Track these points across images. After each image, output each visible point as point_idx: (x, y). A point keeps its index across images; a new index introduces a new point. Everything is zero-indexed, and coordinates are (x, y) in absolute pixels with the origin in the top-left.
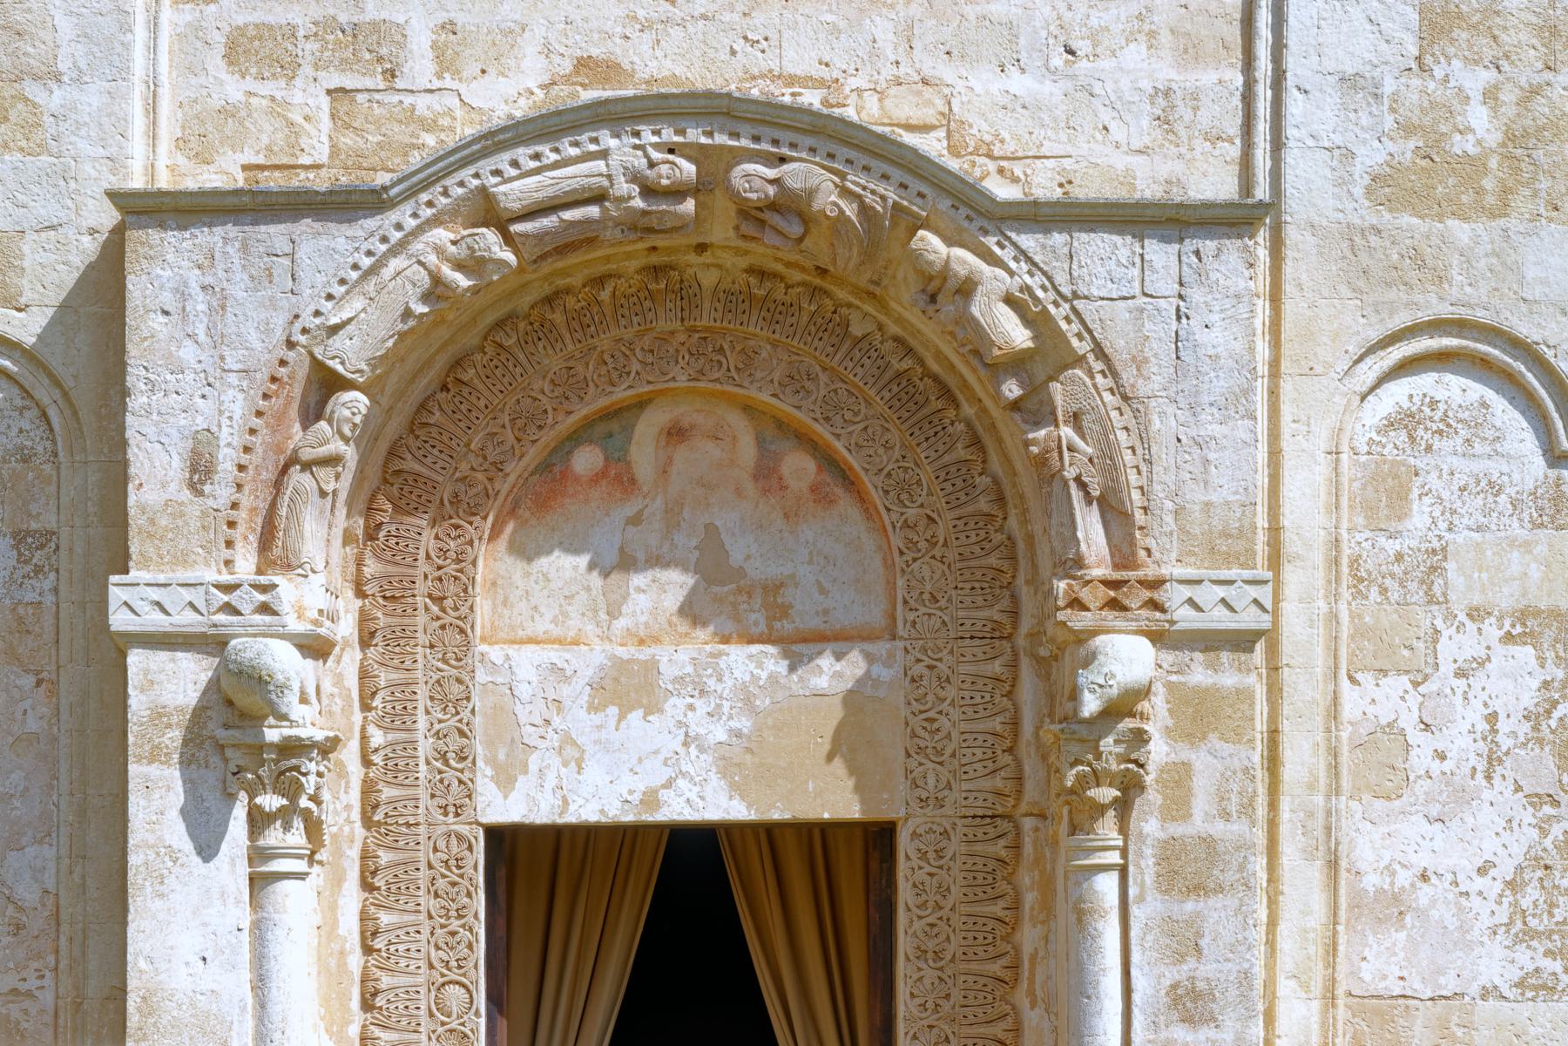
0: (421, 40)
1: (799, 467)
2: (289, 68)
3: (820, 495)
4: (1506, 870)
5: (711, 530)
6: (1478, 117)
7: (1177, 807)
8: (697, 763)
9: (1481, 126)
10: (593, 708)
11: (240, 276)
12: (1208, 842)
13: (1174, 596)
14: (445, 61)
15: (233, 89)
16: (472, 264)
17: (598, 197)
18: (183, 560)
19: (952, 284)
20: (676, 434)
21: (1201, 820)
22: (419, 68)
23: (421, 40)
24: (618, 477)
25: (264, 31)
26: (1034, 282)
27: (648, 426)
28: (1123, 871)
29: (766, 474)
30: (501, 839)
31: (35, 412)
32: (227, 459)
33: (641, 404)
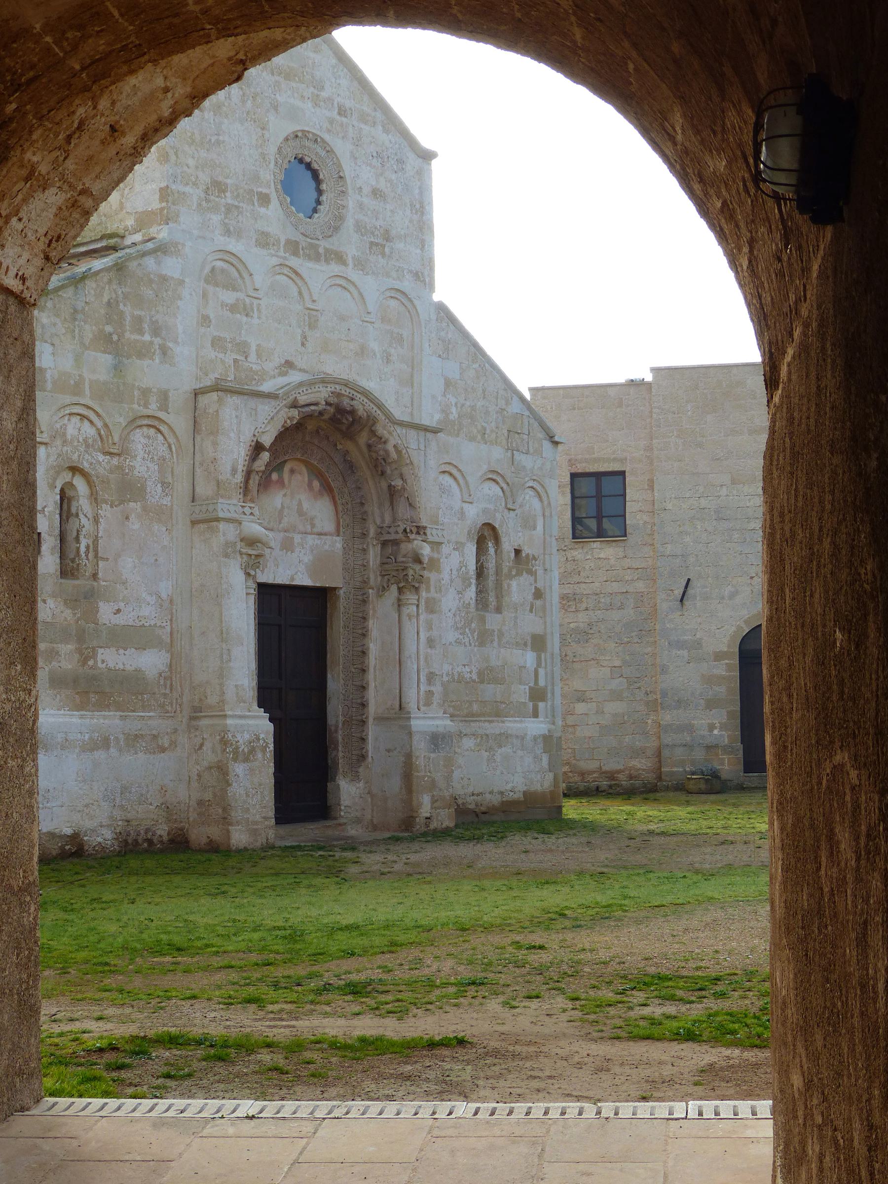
0: (254, 348)
1: (316, 484)
2: (224, 350)
4: (453, 611)
5: (300, 500)
6: (454, 410)
7: (428, 590)
9: (454, 413)
10: (281, 550)
11: (244, 414)
12: (434, 599)
13: (428, 532)
14: (259, 356)
15: (212, 354)
17: (316, 404)
18: (229, 498)
19: (383, 440)
20: (292, 471)
21: (433, 594)
22: (253, 357)
23: (254, 348)
24: (281, 483)
25: (220, 339)
26: (400, 442)
27: (287, 468)
28: (418, 606)
31: (166, 445)
33: (285, 461)
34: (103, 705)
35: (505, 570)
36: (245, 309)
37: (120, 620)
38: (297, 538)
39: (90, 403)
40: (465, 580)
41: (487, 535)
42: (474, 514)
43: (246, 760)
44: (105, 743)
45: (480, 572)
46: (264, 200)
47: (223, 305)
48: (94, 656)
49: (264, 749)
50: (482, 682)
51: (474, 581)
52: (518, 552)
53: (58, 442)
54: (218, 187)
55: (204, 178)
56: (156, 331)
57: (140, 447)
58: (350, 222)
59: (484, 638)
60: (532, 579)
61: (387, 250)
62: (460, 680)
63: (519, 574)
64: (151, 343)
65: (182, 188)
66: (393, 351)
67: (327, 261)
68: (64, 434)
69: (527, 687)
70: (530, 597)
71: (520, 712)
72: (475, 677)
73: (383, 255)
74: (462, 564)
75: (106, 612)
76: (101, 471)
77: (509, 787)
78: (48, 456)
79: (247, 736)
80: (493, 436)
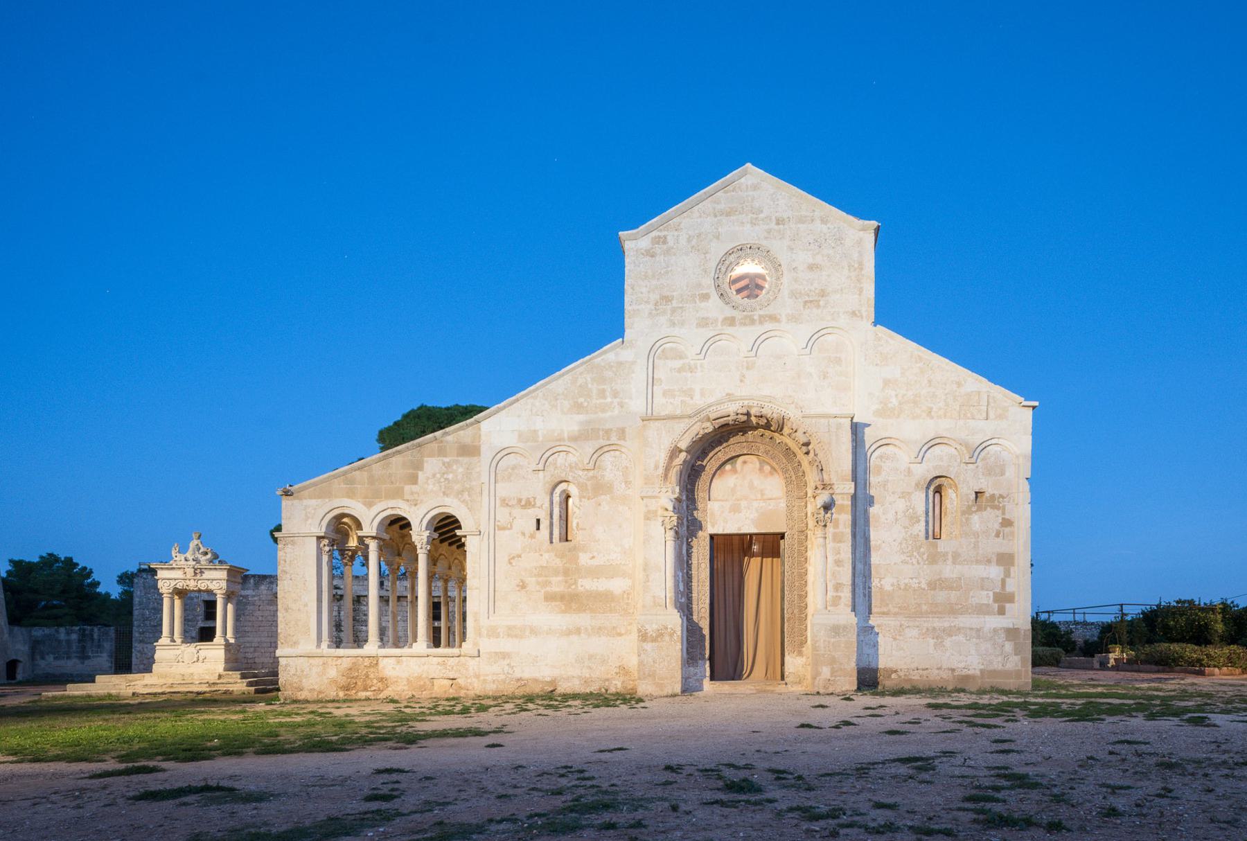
3: (771, 474)
24: (734, 471)
29: (761, 469)
30: (712, 537)
34: (582, 609)
37: (594, 562)
43: (654, 640)
44: (578, 631)
46: (705, 297)
48: (575, 583)
49: (671, 635)
54: (667, 299)
55: (655, 297)
56: (615, 394)
59: (934, 559)
60: (999, 513)
61: (822, 303)
65: (636, 307)
67: (761, 323)
69: (991, 594)
70: (997, 526)
71: (981, 610)
72: (924, 586)
73: (818, 306)
75: (584, 559)
77: (962, 665)
79: (655, 626)
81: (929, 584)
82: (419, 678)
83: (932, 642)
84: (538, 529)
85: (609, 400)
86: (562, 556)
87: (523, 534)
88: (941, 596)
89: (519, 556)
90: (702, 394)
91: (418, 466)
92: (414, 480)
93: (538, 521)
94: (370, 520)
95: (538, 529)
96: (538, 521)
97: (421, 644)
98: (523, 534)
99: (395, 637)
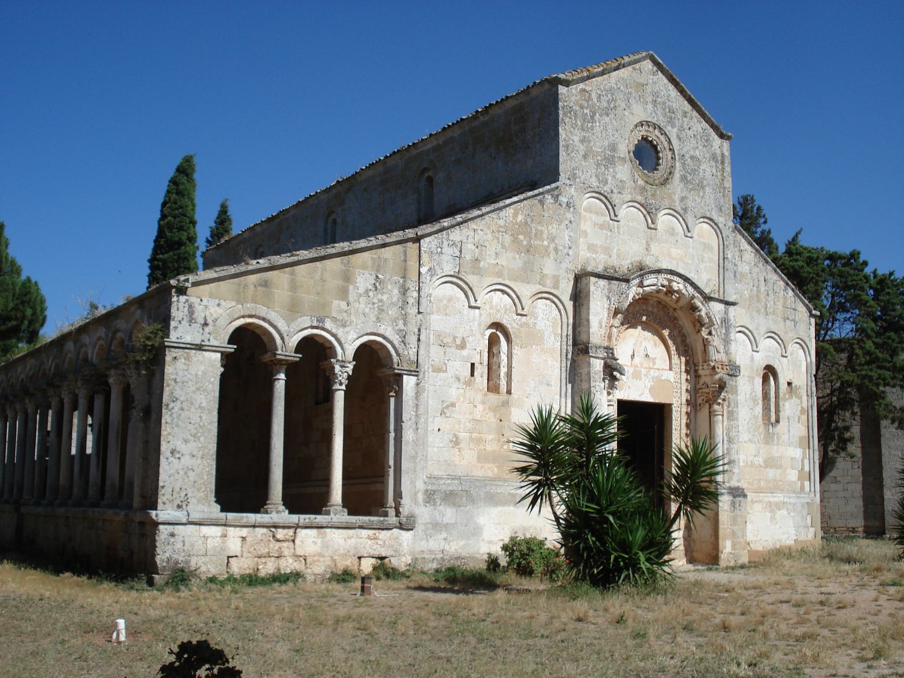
8: (647, 391)
16: (638, 294)
32: (604, 324)
35: (781, 395)
36: (609, 227)
38: (644, 371)
39: (507, 282)
40: (755, 400)
41: (770, 372)
42: (761, 360)
45: (766, 396)
47: (595, 224)
50: (766, 467)
51: (760, 402)
52: (789, 384)
53: (488, 307)
57: (540, 311)
58: (677, 175)
60: (799, 401)
61: (701, 194)
62: (752, 465)
63: (791, 397)
64: (548, 246)
66: (705, 255)
68: (491, 302)
70: (798, 413)
72: (762, 464)
74: (753, 390)
76: (515, 325)
78: (481, 315)
80: (772, 310)
81: (765, 462)
82: (345, 556)
83: (769, 515)
84: (472, 374)
85: (546, 243)
86: (494, 409)
87: (459, 379)
88: (771, 473)
89: (453, 405)
90: (618, 256)
91: (347, 278)
92: (343, 294)
93: (473, 365)
94: (288, 337)
95: (472, 374)
96: (473, 365)
97: (337, 512)
98: (459, 379)
99: (306, 498)
